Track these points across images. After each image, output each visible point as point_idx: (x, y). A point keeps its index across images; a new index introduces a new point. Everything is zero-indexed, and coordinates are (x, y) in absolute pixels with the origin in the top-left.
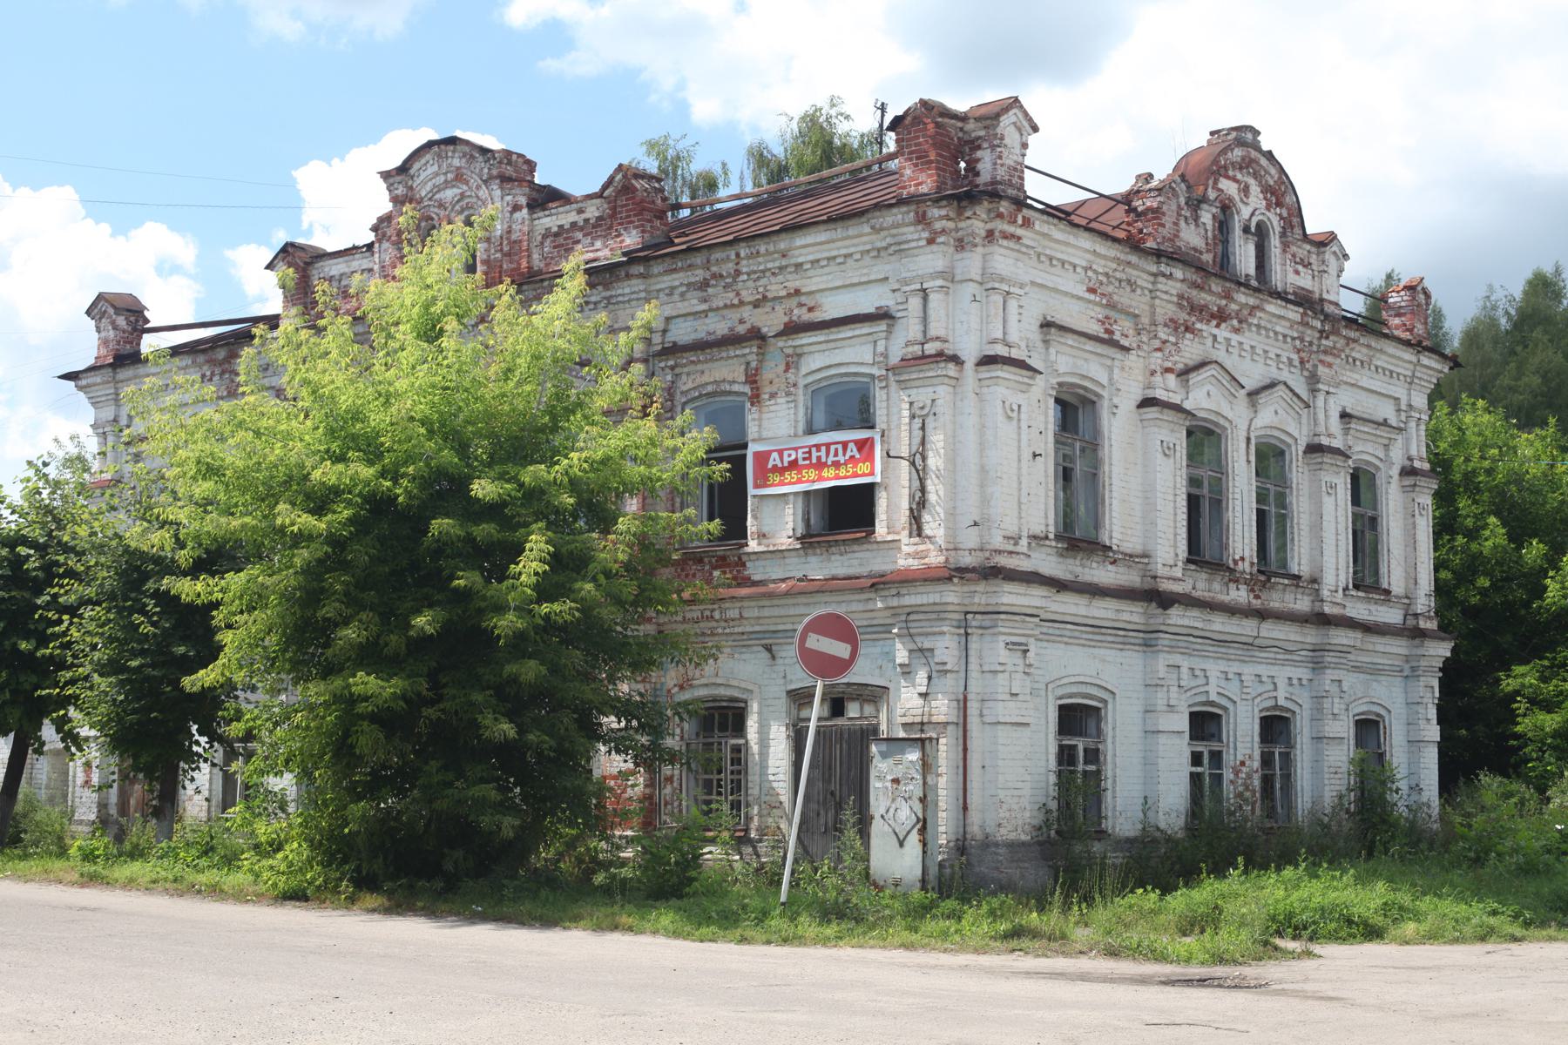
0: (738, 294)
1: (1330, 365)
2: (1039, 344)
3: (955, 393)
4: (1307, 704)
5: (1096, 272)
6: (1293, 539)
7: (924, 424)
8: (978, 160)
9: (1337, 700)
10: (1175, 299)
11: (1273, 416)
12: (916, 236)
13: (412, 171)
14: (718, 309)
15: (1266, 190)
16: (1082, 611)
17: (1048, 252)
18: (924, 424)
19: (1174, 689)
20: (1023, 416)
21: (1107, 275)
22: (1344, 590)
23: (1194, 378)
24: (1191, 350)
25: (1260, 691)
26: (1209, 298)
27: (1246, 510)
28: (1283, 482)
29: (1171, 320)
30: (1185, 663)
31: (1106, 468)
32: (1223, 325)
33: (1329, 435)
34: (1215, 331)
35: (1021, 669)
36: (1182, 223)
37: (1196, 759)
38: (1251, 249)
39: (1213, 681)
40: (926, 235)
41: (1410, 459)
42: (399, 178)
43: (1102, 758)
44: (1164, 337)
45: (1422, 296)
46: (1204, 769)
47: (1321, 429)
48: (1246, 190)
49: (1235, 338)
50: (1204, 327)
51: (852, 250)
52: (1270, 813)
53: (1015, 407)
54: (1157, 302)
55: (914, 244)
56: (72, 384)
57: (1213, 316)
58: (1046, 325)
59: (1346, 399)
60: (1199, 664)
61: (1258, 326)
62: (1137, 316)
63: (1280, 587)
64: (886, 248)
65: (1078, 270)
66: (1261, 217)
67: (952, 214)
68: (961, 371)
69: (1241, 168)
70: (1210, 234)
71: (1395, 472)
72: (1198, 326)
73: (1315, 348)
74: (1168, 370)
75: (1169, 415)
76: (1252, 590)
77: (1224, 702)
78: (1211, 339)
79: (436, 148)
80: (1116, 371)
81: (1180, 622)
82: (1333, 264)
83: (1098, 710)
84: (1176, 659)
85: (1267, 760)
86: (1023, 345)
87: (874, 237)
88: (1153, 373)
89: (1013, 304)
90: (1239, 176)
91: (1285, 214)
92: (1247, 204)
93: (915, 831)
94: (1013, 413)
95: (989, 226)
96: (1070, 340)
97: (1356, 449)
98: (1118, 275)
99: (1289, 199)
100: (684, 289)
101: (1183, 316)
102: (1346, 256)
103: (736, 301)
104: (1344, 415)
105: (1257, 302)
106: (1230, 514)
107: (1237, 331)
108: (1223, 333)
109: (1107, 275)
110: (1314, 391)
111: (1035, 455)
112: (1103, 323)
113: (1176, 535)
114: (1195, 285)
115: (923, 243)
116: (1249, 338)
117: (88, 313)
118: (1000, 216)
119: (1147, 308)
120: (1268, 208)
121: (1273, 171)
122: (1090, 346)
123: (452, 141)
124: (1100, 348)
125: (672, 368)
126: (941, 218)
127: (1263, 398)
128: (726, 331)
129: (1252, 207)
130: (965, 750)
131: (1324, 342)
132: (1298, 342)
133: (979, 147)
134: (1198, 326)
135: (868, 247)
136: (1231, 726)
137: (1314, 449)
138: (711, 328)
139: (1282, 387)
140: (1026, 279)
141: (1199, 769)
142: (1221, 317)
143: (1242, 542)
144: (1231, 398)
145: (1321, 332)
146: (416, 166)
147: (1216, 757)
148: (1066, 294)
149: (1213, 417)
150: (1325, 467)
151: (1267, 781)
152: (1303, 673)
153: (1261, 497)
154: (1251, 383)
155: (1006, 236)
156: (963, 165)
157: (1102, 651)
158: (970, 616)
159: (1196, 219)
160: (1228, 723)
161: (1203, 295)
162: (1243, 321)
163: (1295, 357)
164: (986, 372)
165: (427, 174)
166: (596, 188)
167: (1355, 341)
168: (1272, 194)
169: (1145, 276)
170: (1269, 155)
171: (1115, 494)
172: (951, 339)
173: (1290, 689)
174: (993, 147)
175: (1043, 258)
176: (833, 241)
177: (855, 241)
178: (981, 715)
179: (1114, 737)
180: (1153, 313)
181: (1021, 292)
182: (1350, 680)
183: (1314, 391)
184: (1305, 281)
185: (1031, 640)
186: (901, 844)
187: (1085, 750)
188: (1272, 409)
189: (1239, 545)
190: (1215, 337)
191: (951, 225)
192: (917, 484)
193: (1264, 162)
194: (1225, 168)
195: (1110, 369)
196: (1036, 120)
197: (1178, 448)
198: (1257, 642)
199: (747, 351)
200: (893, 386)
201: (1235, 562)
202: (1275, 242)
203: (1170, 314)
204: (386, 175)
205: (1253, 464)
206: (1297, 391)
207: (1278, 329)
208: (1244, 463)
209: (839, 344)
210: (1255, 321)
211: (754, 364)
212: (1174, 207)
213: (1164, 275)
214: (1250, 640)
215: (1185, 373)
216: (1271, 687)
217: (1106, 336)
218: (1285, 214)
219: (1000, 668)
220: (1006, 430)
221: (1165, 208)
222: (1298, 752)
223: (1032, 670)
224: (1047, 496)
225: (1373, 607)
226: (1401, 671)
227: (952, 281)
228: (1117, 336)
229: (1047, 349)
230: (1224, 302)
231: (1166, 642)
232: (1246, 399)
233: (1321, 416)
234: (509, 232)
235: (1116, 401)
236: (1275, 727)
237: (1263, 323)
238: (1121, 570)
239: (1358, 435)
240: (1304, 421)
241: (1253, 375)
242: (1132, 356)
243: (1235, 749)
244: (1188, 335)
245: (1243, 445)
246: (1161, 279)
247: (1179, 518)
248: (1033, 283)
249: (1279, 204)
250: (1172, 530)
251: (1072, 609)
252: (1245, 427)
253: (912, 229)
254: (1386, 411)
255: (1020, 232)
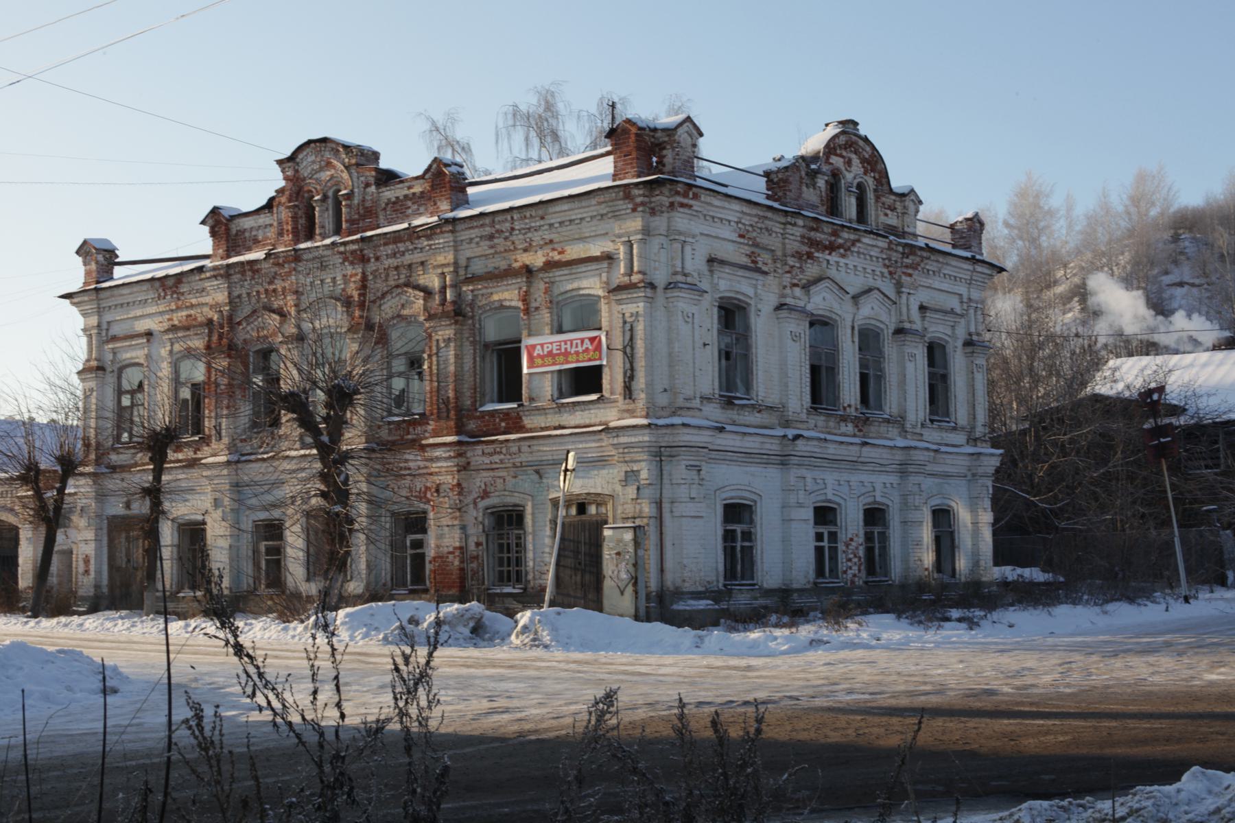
0: (513, 243)
1: (910, 275)
2: (707, 273)
3: (651, 307)
4: (897, 500)
5: (744, 224)
6: (885, 391)
7: (632, 326)
8: (664, 156)
9: (917, 497)
10: (799, 239)
11: (871, 310)
12: (624, 207)
13: (298, 160)
14: (501, 252)
15: (863, 161)
16: (738, 443)
17: (711, 213)
18: (632, 326)
19: (802, 492)
20: (695, 321)
21: (751, 225)
22: (922, 425)
23: (813, 289)
24: (812, 270)
25: (863, 491)
26: (823, 236)
27: (852, 374)
28: (879, 357)
29: (797, 252)
30: (809, 475)
31: (754, 350)
32: (834, 254)
33: (910, 322)
34: (828, 257)
35: (697, 482)
36: (804, 188)
37: (819, 537)
38: (853, 201)
39: (830, 487)
40: (630, 206)
41: (970, 334)
42: (289, 164)
43: (753, 537)
44: (792, 263)
45: (978, 225)
46: (825, 544)
47: (905, 317)
48: (849, 163)
49: (842, 261)
50: (820, 255)
51: (585, 215)
52: (871, 570)
53: (690, 315)
54: (787, 241)
55: (623, 212)
56: (67, 302)
57: (826, 248)
58: (711, 260)
59: (923, 296)
60: (818, 474)
61: (858, 253)
62: (773, 251)
63: (876, 424)
64: (606, 214)
65: (732, 223)
66: (860, 180)
67: (647, 193)
68: (655, 292)
69: (845, 149)
70: (823, 194)
71: (959, 343)
72: (816, 254)
73: (899, 264)
74: (795, 285)
75: (794, 315)
76: (857, 426)
77: (837, 499)
78: (825, 262)
79: (313, 145)
80: (760, 287)
81: (805, 449)
82: (912, 207)
83: (750, 506)
84: (803, 472)
85: (869, 537)
86: (695, 274)
87: (598, 207)
88: (785, 287)
89: (688, 249)
90: (844, 153)
91: (877, 177)
92: (850, 172)
93: (630, 585)
94: (689, 318)
95: (671, 200)
96: (727, 269)
97: (931, 329)
98: (759, 225)
99: (879, 167)
100: (478, 239)
101: (805, 249)
102: (920, 202)
103: (512, 248)
104: (922, 308)
105: (857, 237)
106: (841, 376)
107: (843, 256)
108: (834, 258)
109: (751, 225)
110: (899, 293)
111: (705, 345)
112: (750, 256)
113: (801, 392)
114: (812, 229)
115: (629, 211)
116: (852, 261)
117: (77, 253)
118: (678, 193)
119: (780, 245)
120: (865, 173)
121: (868, 149)
122: (741, 272)
123: (324, 140)
124: (748, 274)
125: (472, 291)
126: (640, 195)
127: (862, 300)
128: (506, 267)
129: (854, 173)
130: (661, 534)
131: (905, 260)
132: (887, 262)
133: (664, 148)
134: (816, 254)
135: (595, 213)
136: (843, 515)
137: (899, 331)
138: (497, 265)
139: (876, 291)
140: (697, 231)
141: (821, 544)
142: (832, 248)
143: (849, 391)
144: (840, 301)
145: (903, 254)
146: (300, 156)
147: (833, 536)
148: (724, 239)
149: (828, 314)
150: (907, 343)
151: (869, 551)
152: (893, 479)
153: (863, 365)
154: (852, 291)
155: (682, 205)
156: (655, 159)
157: (752, 469)
158: (662, 449)
159: (814, 185)
160: (841, 513)
161: (818, 235)
162: (847, 249)
163: (885, 271)
164: (670, 294)
165: (308, 162)
166: (420, 172)
167: (928, 258)
168: (868, 163)
169: (778, 225)
170: (866, 140)
171: (759, 368)
172: (648, 272)
173: (885, 490)
174: (673, 149)
175: (708, 218)
176: (572, 210)
177: (586, 210)
178: (672, 512)
179: (761, 524)
180: (784, 248)
181: (693, 241)
182: (928, 482)
183: (899, 293)
184: (892, 220)
185: (703, 463)
186: (622, 593)
187: (743, 533)
188: (870, 306)
189: (847, 397)
190: (828, 261)
191: (646, 199)
192: (628, 366)
193: (861, 143)
194: (835, 149)
195: (755, 287)
196: (703, 130)
197: (802, 335)
198: (860, 460)
199: (519, 280)
200: (613, 303)
201: (845, 408)
202: (870, 196)
203: (796, 248)
204: (280, 162)
205: (857, 344)
206: (887, 293)
207: (872, 253)
208: (849, 342)
209: (578, 275)
210: (856, 249)
211: (524, 289)
212: (798, 178)
213: (790, 224)
214: (855, 459)
215: (806, 287)
216: (872, 489)
217: (752, 265)
218: (877, 177)
219: (683, 482)
220: (685, 329)
221: (791, 179)
222: (891, 531)
223: (704, 483)
224: (713, 371)
225: (944, 435)
226: (965, 476)
227: (649, 235)
228: (760, 265)
229: (712, 276)
230: (833, 238)
231: (796, 462)
232: (851, 301)
233: (904, 310)
234: (363, 201)
235: (759, 306)
236: (874, 516)
237: (861, 250)
238: (765, 416)
239: (933, 320)
240: (893, 313)
241: (854, 283)
242: (770, 277)
243: (846, 530)
244: (809, 261)
245: (849, 331)
246: (789, 226)
247: (803, 381)
248: (701, 234)
249: (872, 170)
250: (799, 389)
251: (732, 443)
252: (850, 320)
253: (621, 202)
254: (954, 303)
255: (691, 202)
